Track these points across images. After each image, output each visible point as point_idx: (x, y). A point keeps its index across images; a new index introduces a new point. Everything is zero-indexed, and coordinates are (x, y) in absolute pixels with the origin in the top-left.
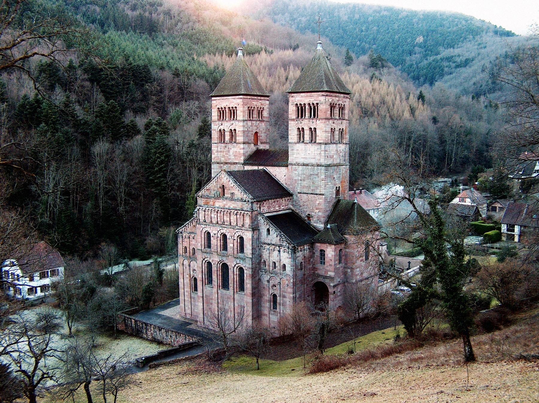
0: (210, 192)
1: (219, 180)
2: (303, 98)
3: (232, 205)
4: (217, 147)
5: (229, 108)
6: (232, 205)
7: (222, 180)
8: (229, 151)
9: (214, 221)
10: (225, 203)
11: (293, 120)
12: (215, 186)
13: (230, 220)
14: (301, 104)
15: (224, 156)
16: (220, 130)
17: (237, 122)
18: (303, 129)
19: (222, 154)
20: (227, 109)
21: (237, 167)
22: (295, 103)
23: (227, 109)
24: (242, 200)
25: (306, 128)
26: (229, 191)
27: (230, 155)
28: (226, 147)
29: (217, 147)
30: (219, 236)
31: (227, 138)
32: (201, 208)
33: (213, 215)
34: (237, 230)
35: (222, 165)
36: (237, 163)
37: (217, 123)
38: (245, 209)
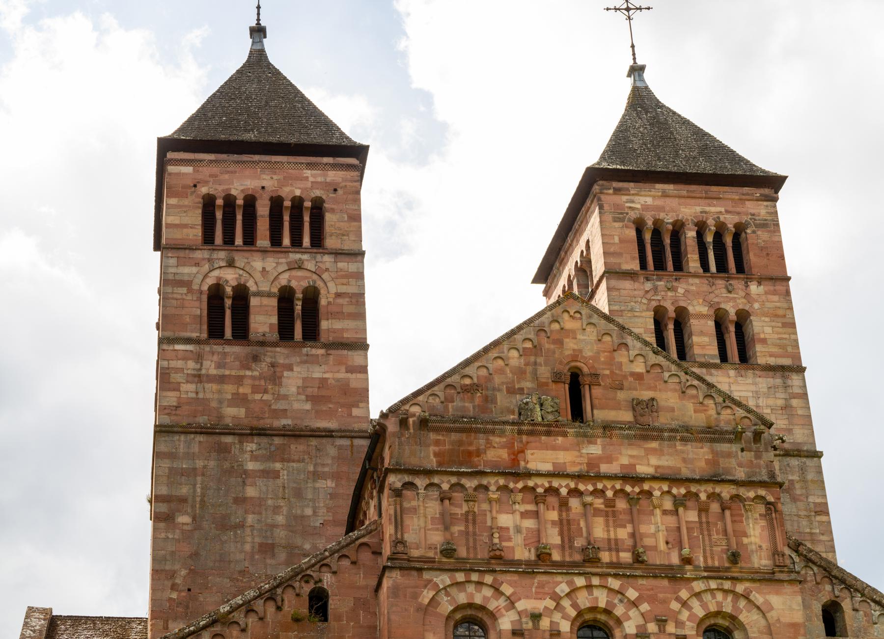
1: (547, 346)
3: (648, 460)
4: (199, 358)
5: (276, 203)
6: (648, 460)
7: (570, 345)
8: (275, 379)
9: (523, 553)
10: (595, 450)
12: (520, 373)
13: (633, 535)
15: (239, 400)
17: (328, 259)
19: (229, 389)
20: (263, 210)
21: (332, 451)
23: (263, 210)
24: (712, 434)
26: (621, 395)
27: (285, 397)
28: (256, 358)
29: (199, 358)
30: (565, 627)
31: (263, 319)
32: (421, 482)
33: (505, 520)
34: (698, 586)
35: (228, 439)
36: (329, 434)
37: (198, 255)
38: (740, 474)
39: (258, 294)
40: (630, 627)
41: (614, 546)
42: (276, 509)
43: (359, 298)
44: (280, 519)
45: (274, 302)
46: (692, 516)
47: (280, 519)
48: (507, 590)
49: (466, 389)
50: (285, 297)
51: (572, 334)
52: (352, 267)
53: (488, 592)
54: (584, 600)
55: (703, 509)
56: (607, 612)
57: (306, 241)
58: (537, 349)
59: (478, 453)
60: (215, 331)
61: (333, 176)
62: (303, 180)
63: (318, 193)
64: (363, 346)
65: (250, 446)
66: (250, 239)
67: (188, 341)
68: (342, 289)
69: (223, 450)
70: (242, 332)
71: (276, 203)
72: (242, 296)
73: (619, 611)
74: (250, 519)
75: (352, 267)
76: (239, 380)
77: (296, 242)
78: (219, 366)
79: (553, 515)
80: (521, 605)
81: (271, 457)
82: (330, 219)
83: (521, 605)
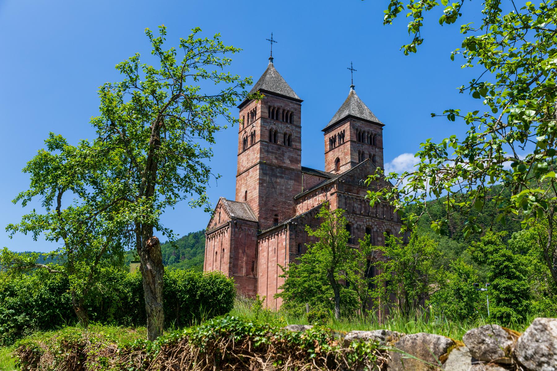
0: (354, 179)
2: (363, 126)
4: (268, 147)
8: (283, 155)
11: (354, 142)
12: (359, 174)
13: (376, 211)
14: (360, 130)
16: (270, 131)
18: (363, 152)
20: (281, 111)
22: (356, 127)
23: (281, 111)
25: (366, 152)
28: (279, 149)
30: (365, 228)
33: (356, 205)
39: (280, 133)
40: (375, 230)
41: (373, 213)
42: (283, 186)
43: (300, 138)
44: (284, 188)
45: (283, 136)
46: (385, 209)
47: (284, 188)
48: (356, 220)
49: (351, 176)
50: (285, 134)
51: (368, 167)
52: (299, 130)
53: (352, 219)
54: (368, 223)
55: (387, 208)
56: (371, 226)
57: (289, 121)
58: (362, 169)
59: (352, 190)
60: (270, 140)
61: (296, 106)
62: (290, 107)
63: (292, 110)
64: (300, 150)
65: (278, 170)
66: (277, 119)
67: (266, 142)
68: (297, 135)
69: (272, 170)
70: (275, 142)
71: (284, 111)
72: (276, 132)
73: (373, 226)
74: (278, 187)
75: (299, 130)
76: (276, 153)
77: (287, 121)
78: (272, 149)
79: (363, 205)
80: (358, 223)
81: (282, 173)
82: (295, 118)
83: (358, 223)
